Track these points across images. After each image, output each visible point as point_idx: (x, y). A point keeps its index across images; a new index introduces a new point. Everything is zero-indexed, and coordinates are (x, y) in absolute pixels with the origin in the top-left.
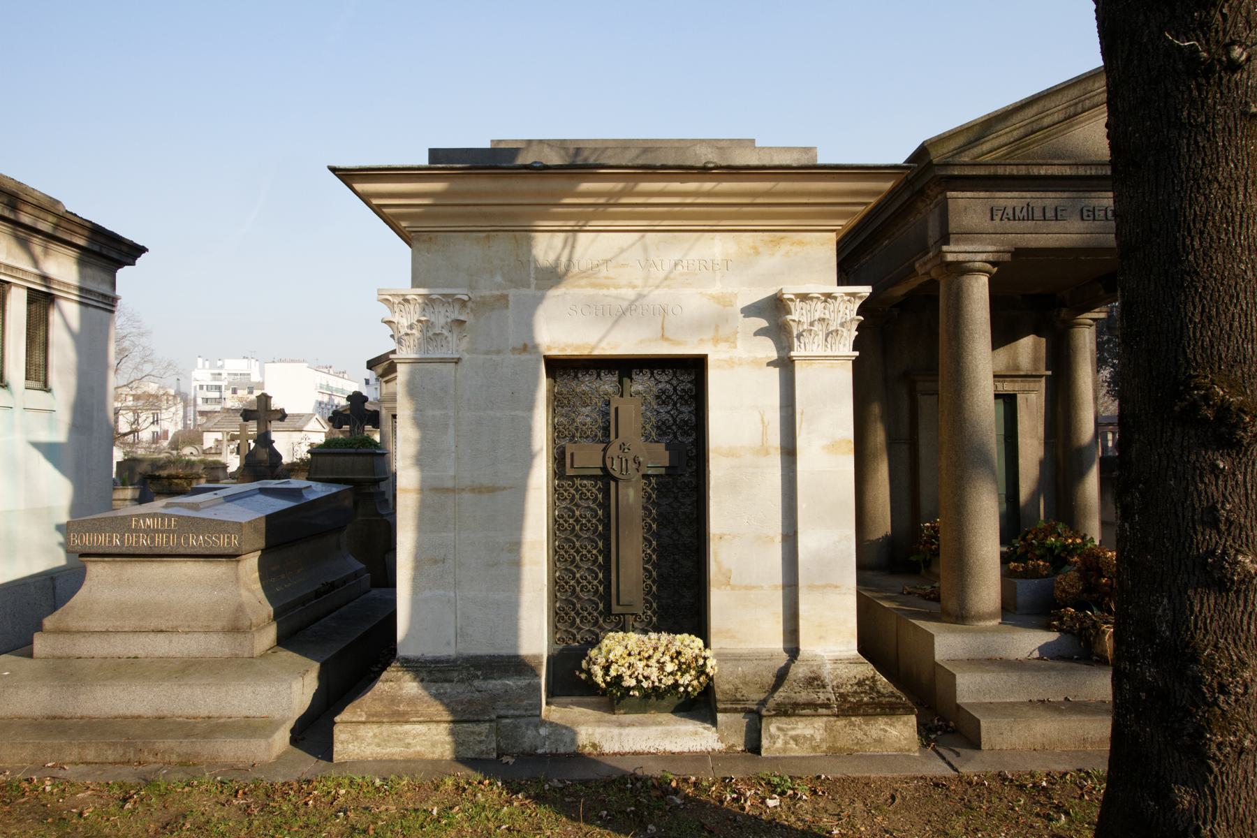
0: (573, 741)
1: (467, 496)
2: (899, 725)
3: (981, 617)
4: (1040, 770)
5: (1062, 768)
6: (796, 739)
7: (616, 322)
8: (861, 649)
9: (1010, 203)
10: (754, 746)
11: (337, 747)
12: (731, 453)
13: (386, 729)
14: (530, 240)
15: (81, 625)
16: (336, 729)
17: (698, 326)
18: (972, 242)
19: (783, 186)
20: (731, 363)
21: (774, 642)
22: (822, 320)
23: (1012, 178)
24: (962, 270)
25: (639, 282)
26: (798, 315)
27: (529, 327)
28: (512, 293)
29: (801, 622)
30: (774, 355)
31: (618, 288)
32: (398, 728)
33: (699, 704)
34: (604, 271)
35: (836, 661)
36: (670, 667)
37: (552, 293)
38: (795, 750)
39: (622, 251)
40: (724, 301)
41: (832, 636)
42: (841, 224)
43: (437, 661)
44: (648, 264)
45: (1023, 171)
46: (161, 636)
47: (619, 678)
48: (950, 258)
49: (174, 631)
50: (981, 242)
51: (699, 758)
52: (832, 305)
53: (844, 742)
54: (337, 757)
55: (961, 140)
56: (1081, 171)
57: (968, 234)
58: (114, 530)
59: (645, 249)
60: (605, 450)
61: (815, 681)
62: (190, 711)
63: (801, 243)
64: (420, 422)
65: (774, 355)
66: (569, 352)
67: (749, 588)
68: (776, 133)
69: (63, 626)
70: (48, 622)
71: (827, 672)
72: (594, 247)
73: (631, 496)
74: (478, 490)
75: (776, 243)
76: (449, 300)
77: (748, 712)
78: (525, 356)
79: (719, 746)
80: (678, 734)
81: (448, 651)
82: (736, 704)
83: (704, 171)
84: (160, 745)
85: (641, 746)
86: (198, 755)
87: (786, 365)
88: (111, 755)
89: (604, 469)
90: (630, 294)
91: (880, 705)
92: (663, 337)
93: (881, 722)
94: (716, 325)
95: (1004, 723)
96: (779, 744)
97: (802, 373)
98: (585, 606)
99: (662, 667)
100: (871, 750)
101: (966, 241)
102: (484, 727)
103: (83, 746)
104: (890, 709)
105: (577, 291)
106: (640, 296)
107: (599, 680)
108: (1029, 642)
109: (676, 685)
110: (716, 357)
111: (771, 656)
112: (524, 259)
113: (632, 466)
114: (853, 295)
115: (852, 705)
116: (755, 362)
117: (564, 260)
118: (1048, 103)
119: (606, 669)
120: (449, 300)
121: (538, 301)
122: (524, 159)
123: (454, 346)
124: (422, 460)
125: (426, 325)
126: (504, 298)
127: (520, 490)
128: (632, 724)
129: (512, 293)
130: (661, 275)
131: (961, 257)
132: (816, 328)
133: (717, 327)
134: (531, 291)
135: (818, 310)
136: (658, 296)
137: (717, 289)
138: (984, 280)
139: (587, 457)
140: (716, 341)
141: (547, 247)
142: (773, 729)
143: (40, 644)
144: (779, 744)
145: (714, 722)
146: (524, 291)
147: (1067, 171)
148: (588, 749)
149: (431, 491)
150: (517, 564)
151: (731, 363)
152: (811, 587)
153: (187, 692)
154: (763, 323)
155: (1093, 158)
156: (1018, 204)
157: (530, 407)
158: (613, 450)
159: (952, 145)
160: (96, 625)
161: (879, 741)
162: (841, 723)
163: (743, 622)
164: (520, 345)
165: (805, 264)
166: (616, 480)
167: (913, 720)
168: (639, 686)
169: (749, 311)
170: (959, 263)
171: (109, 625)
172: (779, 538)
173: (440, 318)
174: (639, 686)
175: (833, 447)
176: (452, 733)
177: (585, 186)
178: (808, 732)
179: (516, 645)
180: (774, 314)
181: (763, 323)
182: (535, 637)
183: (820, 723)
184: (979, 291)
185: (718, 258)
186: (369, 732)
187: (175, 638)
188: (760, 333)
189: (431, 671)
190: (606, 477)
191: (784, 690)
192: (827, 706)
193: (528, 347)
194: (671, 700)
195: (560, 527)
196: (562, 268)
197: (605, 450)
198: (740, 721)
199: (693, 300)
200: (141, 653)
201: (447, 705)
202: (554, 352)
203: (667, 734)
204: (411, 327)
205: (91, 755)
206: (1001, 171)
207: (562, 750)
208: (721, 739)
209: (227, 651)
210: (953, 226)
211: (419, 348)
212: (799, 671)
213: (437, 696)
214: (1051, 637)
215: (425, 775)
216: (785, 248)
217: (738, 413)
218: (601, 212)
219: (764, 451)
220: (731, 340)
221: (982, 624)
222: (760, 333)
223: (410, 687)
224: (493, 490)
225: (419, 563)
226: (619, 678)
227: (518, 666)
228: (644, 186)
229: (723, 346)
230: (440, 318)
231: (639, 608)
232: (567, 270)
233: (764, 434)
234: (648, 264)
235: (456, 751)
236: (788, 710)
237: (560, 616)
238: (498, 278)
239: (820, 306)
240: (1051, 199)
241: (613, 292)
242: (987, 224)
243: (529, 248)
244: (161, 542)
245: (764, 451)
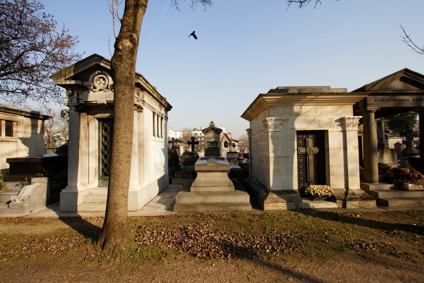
0: (309, 206)
1: (282, 158)
2: (373, 202)
3: (376, 182)
4: (404, 210)
5: (408, 209)
6: (353, 205)
7: (310, 124)
8: (361, 188)
9: (379, 98)
10: (344, 206)
11: (265, 208)
12: (333, 149)
13: (274, 204)
14: (293, 107)
15: (199, 185)
16: (264, 204)
17: (326, 124)
18: (372, 106)
19: (346, 96)
20: (333, 131)
21: (342, 186)
22: (352, 123)
23: (381, 93)
24: (370, 112)
25: (314, 115)
26: (347, 121)
27: (293, 124)
28: (290, 118)
29: (349, 183)
30: (341, 130)
31: (310, 117)
32: (276, 204)
33: (332, 199)
34: (307, 113)
35: (357, 190)
36: (327, 191)
37: (298, 118)
38: (353, 207)
39: (311, 109)
40: (331, 119)
41: (355, 185)
42: (354, 103)
43: (278, 191)
44: (316, 112)
45: (383, 92)
46: (216, 187)
47: (317, 194)
48: (368, 109)
49: (218, 186)
50: (373, 106)
51: (335, 209)
52: (354, 120)
53: (362, 205)
54: (265, 210)
55: (371, 86)
56: (395, 92)
57: (371, 105)
58: (204, 166)
59: (315, 109)
60: (306, 149)
61: (353, 194)
62: (230, 201)
63: (346, 107)
64: (274, 144)
65: (341, 130)
66: (301, 130)
67: (337, 176)
68: (336, 85)
69: (196, 185)
70: (193, 185)
71: (355, 192)
72: (306, 108)
73: (311, 158)
74: (284, 157)
75: (341, 107)
76: (280, 120)
77: (342, 200)
78: (293, 130)
79: (337, 207)
80: (329, 204)
81: (280, 189)
82: (340, 199)
83: (332, 94)
84: (230, 207)
85: (322, 207)
86: (238, 209)
87: (344, 132)
88: (221, 210)
89: (306, 153)
90: (313, 118)
91: (368, 198)
92: (320, 127)
93: (369, 201)
94: (330, 124)
95: (393, 201)
96: (350, 206)
97: (348, 134)
98: (304, 179)
99: (325, 191)
100: (368, 207)
101: (370, 106)
102: (293, 203)
103: (215, 208)
104: (371, 199)
105: (302, 117)
106: (315, 118)
107: (313, 194)
108: (388, 186)
109: (328, 195)
110: (330, 130)
111: (343, 189)
112: (292, 112)
113: (312, 152)
114: (359, 118)
115: (363, 198)
116: (338, 131)
117: (300, 111)
118: (388, 78)
119: (314, 192)
120: (280, 120)
121: (295, 119)
122: (290, 92)
123: (280, 129)
124: (274, 151)
125: (275, 125)
126: (288, 119)
127: (293, 157)
128: (319, 203)
129: (290, 118)
130: (319, 114)
131: (370, 109)
132: (351, 124)
133: (330, 124)
134: (294, 118)
135: (351, 121)
136: (318, 118)
137: (330, 117)
138: (374, 114)
139: (303, 150)
140: (330, 127)
141: (296, 109)
142: (348, 203)
143: (192, 189)
144: (350, 206)
145: (336, 202)
146: (292, 117)
147: (392, 92)
148: (312, 208)
149: (276, 158)
150: (292, 172)
151: (333, 131)
152: (351, 176)
153: (229, 198)
154: (339, 123)
155: (396, 89)
156: (381, 98)
157: (294, 141)
158: (308, 149)
159: (370, 87)
160: (202, 185)
161: (369, 205)
162: (361, 202)
163: (336, 183)
164: (291, 128)
165: (347, 111)
166: (308, 155)
167: (375, 201)
168: (321, 195)
169: (336, 121)
170: (370, 110)
171: (205, 185)
172: (343, 166)
173: (278, 123)
174: (321, 195)
175: (354, 148)
176: (287, 204)
177: (308, 97)
178: (355, 204)
179: (292, 188)
180: (342, 122)
181: (339, 123)
182: (295, 186)
183: (357, 202)
184: (373, 115)
185: (330, 111)
186: (271, 205)
187: (219, 188)
188: (338, 125)
189: (279, 193)
190: (306, 154)
191: (346, 196)
192: (358, 198)
193: (293, 129)
194: (324, 198)
195: (299, 164)
196: (299, 113)
197: (306, 149)
198: (341, 202)
199: (325, 119)
200: (212, 191)
201: (285, 199)
202: (298, 130)
203: (327, 204)
204: (272, 125)
205: (217, 209)
206: (379, 92)
207: (307, 208)
208: (338, 205)
209: (229, 190)
210: (368, 103)
211: (273, 129)
212: (350, 192)
213: (281, 198)
214: (392, 185)
215: (280, 213)
216: (343, 108)
217: (334, 141)
218: (309, 102)
219: (340, 149)
220: (333, 127)
221: (376, 183)
222: (338, 125)
223: (275, 196)
224: (287, 157)
225: (274, 172)
226: (317, 194)
227: (293, 192)
228: (319, 97)
229: (331, 128)
230: (278, 123)
231: (313, 180)
232: (300, 113)
233: (340, 145)
234: (316, 112)
235: (288, 208)
236: (351, 199)
237: (299, 181)
238: (287, 115)
239: (352, 120)
240: (387, 97)
241: (309, 117)
242: (375, 103)
243: (293, 109)
244: (214, 168)
245: (340, 149)
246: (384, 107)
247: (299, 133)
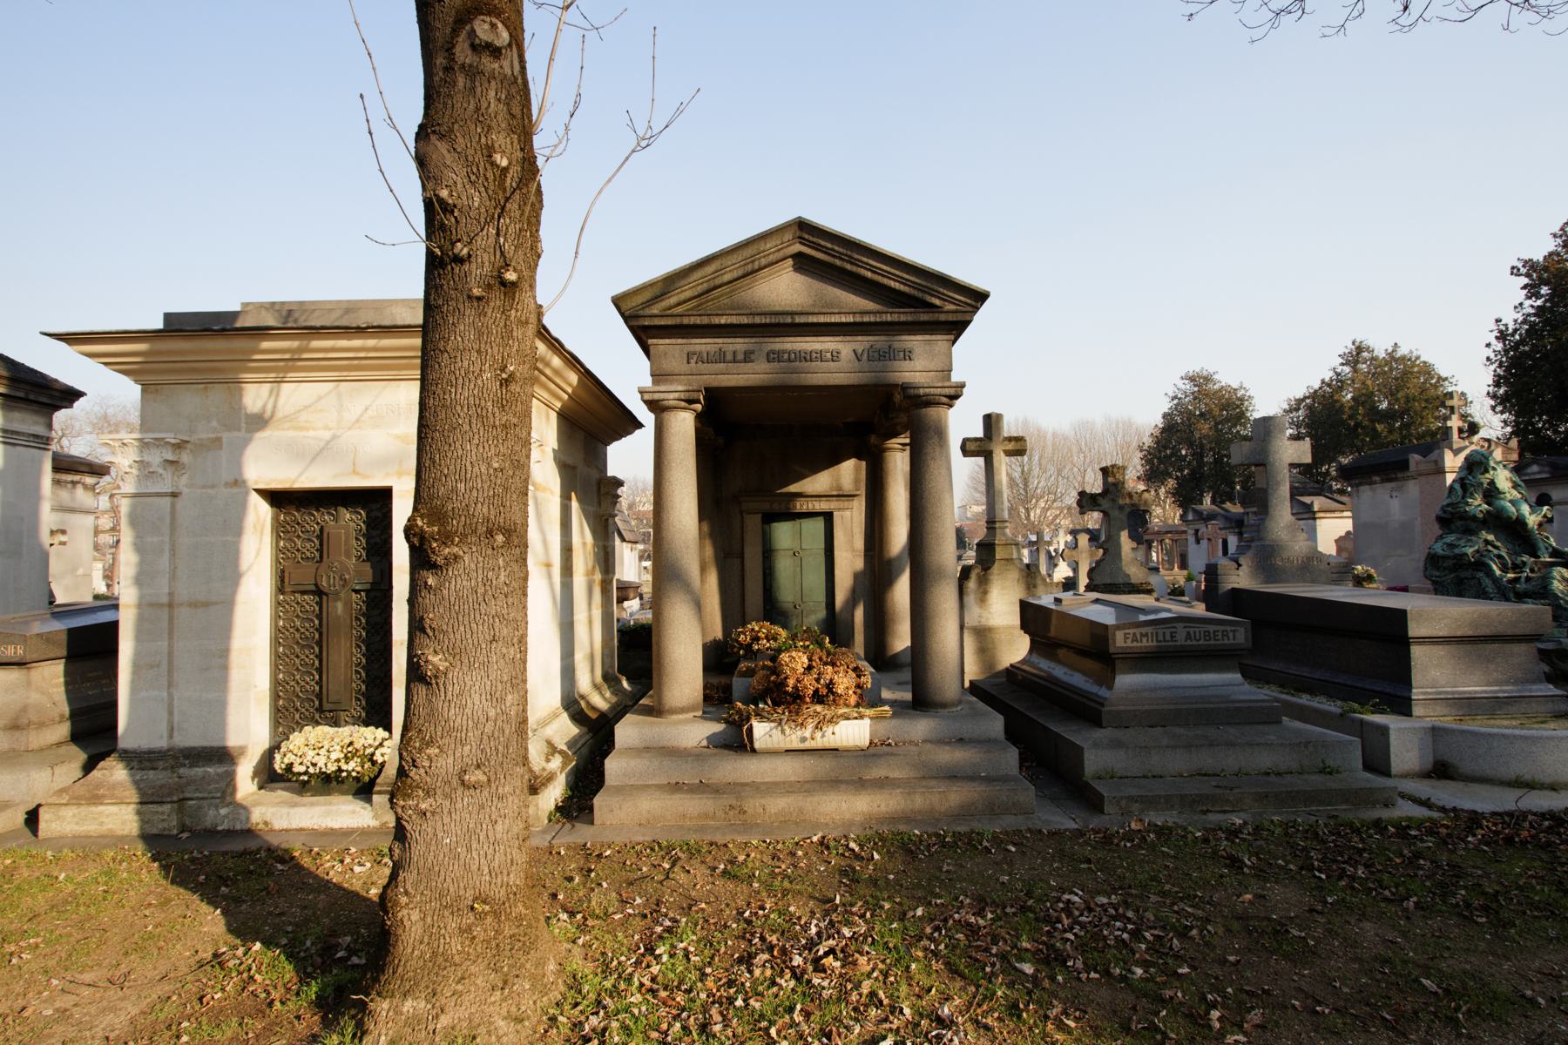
0: (248, 819)
13: (84, 810)
14: (241, 389)
18: (671, 382)
27: (237, 464)
28: (226, 436)
32: (93, 809)
34: (303, 417)
37: (259, 435)
39: (320, 398)
43: (150, 752)
45: (705, 321)
55: (647, 295)
56: (757, 320)
64: (139, 547)
72: (297, 395)
78: (235, 490)
79: (374, 823)
90: (327, 435)
92: (355, 472)
102: (167, 808)
106: (334, 437)
117: (270, 406)
120: (160, 443)
121: (246, 442)
124: (140, 580)
125: (142, 464)
126: (219, 439)
129: (226, 436)
134: (242, 434)
145: (369, 801)
146: (236, 434)
147: (745, 320)
148: (261, 826)
155: (777, 309)
159: (640, 299)
173: (155, 458)
176: (139, 813)
177: (266, 345)
179: (224, 739)
186: (69, 812)
189: (138, 760)
196: (268, 414)
206: (686, 321)
207: (238, 827)
208: (376, 817)
214: (718, 727)
221: (674, 717)
224: (206, 604)
225: (137, 667)
228: (316, 344)
230: (155, 458)
235: (141, 828)
238: (214, 423)
240: (739, 344)
241: (311, 433)
242: (685, 368)
246: (832, 382)
247: (278, 498)
